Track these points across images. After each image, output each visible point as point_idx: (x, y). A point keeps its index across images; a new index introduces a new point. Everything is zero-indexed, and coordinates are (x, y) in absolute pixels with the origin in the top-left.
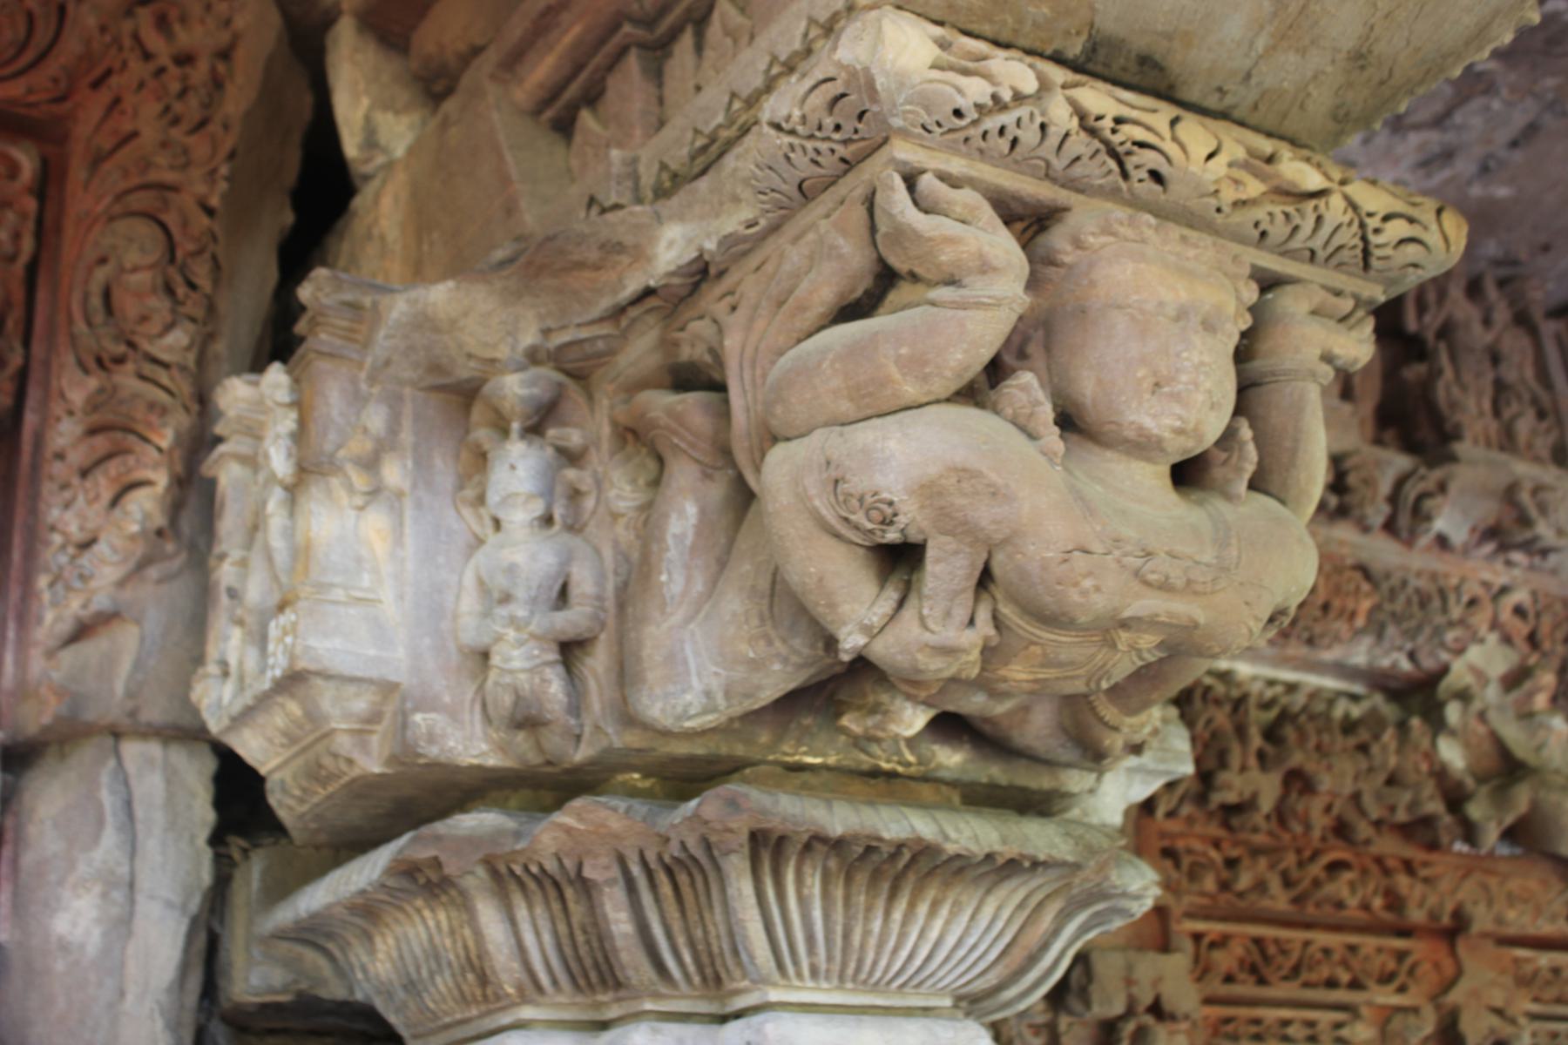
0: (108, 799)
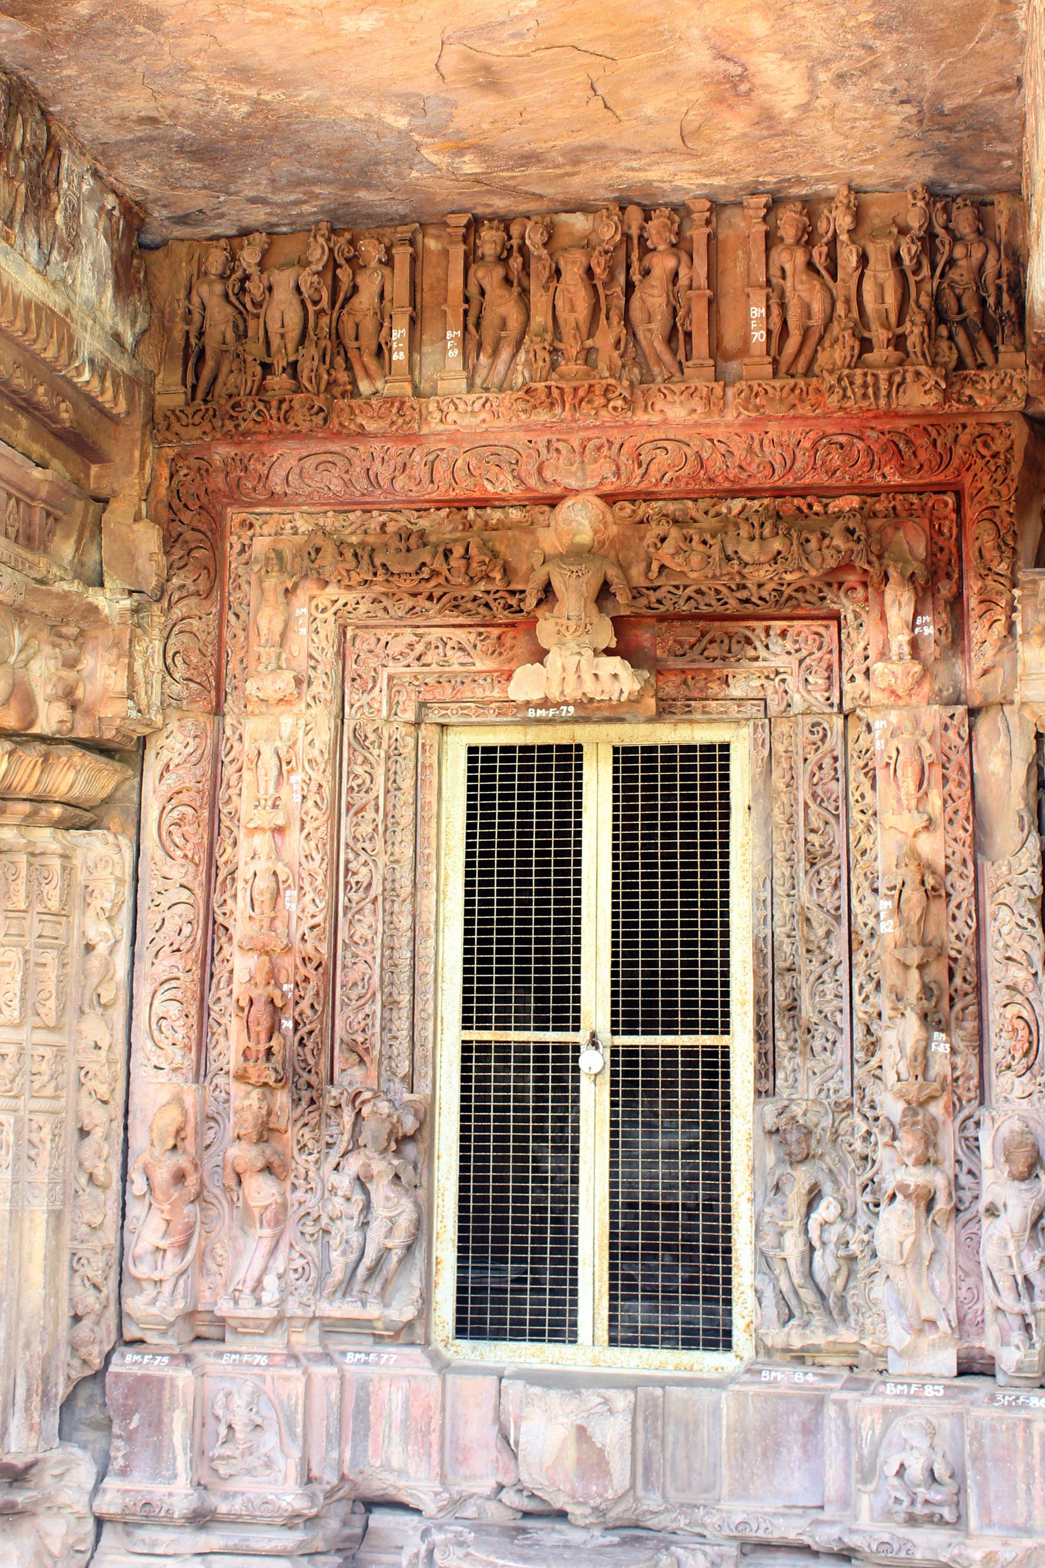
0: (1001, 726)
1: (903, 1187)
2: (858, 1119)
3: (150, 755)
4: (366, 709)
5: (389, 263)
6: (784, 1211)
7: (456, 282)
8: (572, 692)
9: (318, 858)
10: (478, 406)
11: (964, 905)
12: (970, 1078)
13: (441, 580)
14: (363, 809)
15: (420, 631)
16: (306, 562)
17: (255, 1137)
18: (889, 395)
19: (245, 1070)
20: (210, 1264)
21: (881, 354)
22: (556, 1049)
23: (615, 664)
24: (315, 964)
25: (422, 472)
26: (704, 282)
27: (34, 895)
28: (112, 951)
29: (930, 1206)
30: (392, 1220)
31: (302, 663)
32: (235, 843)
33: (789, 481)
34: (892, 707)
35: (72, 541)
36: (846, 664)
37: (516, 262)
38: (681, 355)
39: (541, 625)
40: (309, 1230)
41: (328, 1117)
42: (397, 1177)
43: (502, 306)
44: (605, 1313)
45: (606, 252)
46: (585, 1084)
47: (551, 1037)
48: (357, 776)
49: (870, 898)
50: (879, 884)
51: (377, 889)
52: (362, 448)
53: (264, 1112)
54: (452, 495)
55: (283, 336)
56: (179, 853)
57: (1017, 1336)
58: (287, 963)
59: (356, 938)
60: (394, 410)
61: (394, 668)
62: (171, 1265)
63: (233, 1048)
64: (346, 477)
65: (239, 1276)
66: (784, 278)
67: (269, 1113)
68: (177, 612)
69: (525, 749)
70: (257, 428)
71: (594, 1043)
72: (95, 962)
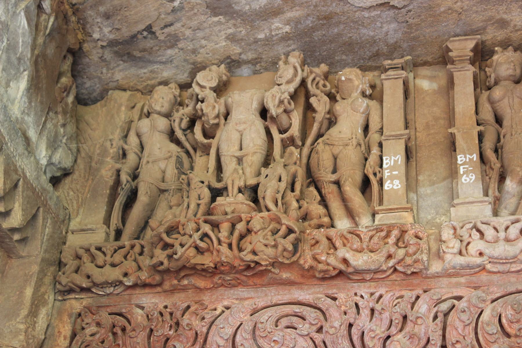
52: (341, 296)
55: (240, 160)
60: (392, 240)
64: (318, 338)
70: (199, 260)
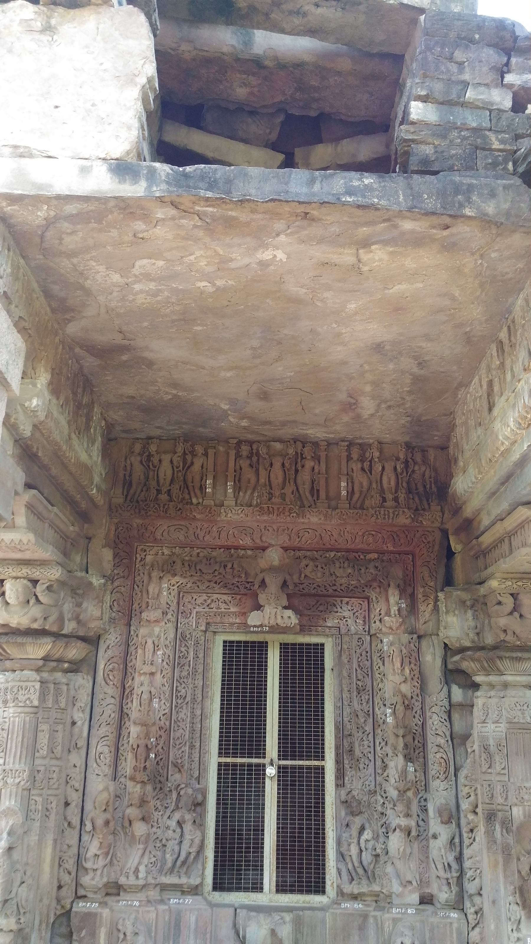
1: (399, 826)
2: (379, 798)
3: (101, 642)
4: (187, 625)
5: (206, 455)
6: (351, 835)
7: (231, 464)
8: (273, 622)
9: (167, 685)
10: (240, 511)
11: (418, 712)
12: (421, 781)
13: (221, 576)
14: (184, 665)
15: (209, 595)
16: (170, 567)
17: (138, 805)
18: (393, 519)
19: (135, 775)
20: (115, 861)
21: (390, 503)
22: (256, 766)
23: (289, 613)
24: (164, 730)
25: (215, 534)
26: (324, 472)
27: (57, 702)
28: (83, 724)
29: (409, 834)
30: (192, 840)
31: (164, 605)
32: (133, 679)
33: (353, 546)
34: (389, 634)
35: (80, 554)
36: (372, 616)
37: (255, 459)
38: (315, 497)
39: (260, 596)
40: (158, 845)
41: (166, 795)
42: (194, 821)
43: (249, 475)
44: (274, 879)
45: (290, 458)
46: (268, 781)
47: (254, 761)
48: (182, 652)
49: (383, 708)
50: (386, 703)
51: (188, 699)
52: (193, 524)
53: (142, 794)
54: (226, 543)
55: (165, 479)
56: (111, 683)
57: (445, 888)
58: (154, 729)
59: (179, 719)
61: (198, 609)
62: (101, 862)
63: (128, 766)
64: (186, 535)
65: (128, 866)
66: (353, 472)
67: (144, 794)
68: (116, 584)
69: (245, 642)
71: (272, 764)
72: (76, 730)
